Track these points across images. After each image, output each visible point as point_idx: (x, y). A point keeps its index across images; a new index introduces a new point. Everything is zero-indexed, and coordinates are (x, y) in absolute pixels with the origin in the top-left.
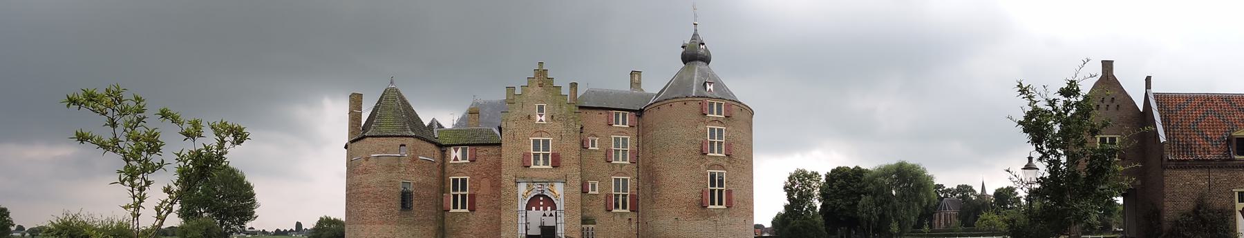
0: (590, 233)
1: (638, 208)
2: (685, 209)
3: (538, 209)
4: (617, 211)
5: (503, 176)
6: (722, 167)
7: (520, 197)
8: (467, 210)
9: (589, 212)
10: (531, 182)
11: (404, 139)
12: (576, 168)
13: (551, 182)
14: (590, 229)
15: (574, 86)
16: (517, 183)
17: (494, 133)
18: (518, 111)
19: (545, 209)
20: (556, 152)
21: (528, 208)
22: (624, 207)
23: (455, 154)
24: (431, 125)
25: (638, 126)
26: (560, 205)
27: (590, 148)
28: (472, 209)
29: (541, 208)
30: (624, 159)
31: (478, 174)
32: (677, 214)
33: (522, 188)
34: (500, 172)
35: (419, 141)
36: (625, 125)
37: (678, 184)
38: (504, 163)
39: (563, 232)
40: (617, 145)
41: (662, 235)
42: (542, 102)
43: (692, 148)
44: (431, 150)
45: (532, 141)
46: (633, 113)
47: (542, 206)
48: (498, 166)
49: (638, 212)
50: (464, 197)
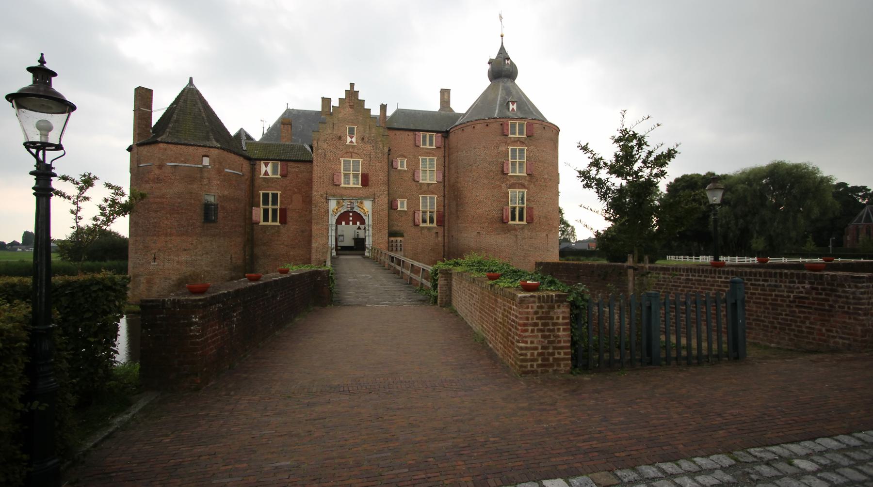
0: (399, 244)
2: (486, 224)
3: (347, 223)
4: (424, 225)
6: (523, 186)
7: (330, 212)
9: (398, 226)
10: (340, 198)
11: (207, 150)
13: (361, 199)
14: (399, 241)
15: (383, 108)
16: (327, 200)
17: (305, 148)
21: (338, 222)
22: (431, 221)
25: (445, 147)
27: (399, 168)
29: (351, 223)
33: (333, 204)
35: (225, 153)
36: (432, 146)
37: (480, 202)
41: (466, 246)
44: (238, 162)
46: (440, 135)
47: (351, 221)
48: (309, 183)
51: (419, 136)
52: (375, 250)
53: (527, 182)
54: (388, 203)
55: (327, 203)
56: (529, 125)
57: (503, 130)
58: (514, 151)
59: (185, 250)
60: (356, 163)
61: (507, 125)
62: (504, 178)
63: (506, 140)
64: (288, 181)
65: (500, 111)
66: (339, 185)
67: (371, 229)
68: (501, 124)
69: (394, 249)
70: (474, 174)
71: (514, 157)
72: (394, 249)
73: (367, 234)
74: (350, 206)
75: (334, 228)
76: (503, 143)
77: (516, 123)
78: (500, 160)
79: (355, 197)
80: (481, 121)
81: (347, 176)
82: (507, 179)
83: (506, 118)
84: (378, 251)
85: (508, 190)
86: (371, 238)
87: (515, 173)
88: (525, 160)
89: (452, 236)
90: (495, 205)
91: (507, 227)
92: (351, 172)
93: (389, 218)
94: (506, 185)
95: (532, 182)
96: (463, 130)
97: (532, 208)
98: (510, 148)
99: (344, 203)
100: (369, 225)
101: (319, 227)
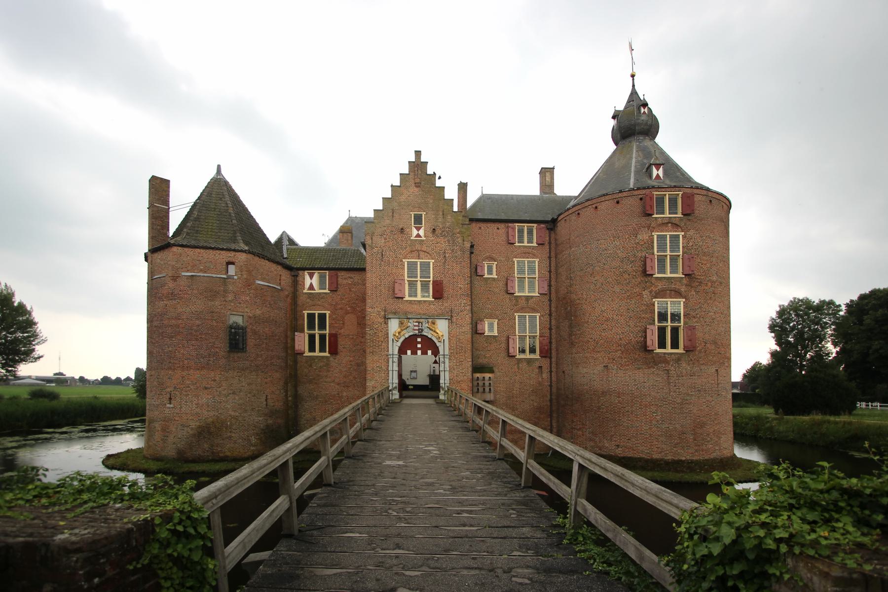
1: (551, 353)
3: (414, 353)
5: (369, 310)
6: (678, 294)
7: (391, 337)
8: (327, 354)
10: (404, 317)
12: (465, 301)
13: (433, 318)
15: (463, 188)
16: (386, 319)
18: (388, 222)
19: (424, 353)
20: (439, 279)
21: (402, 351)
22: (533, 350)
23: (311, 281)
24: (280, 241)
26: (444, 348)
28: (334, 351)
29: (419, 352)
30: (532, 288)
31: (341, 309)
32: (606, 360)
33: (394, 326)
34: (365, 305)
37: (607, 320)
38: (369, 292)
39: (447, 381)
40: (521, 271)
42: (420, 209)
43: (629, 268)
44: (275, 273)
45: (406, 263)
47: (419, 349)
49: (551, 358)
50: (323, 337)
51: (514, 229)
52: (452, 391)
53: (684, 287)
54: (472, 324)
55: (386, 323)
56: (688, 200)
57: (644, 207)
58: (662, 238)
59: (206, 388)
60: (424, 266)
61: (651, 198)
62: (646, 282)
63: (648, 222)
64: (339, 297)
65: (636, 180)
66: (403, 298)
67: (447, 361)
68: (641, 199)
69: (481, 389)
70: (596, 278)
71: (662, 247)
72: (481, 389)
73: (442, 369)
74: (417, 328)
75: (396, 360)
76: (645, 227)
77: (665, 195)
78: (639, 254)
79: (424, 314)
80: (607, 198)
81: (412, 285)
82: (651, 283)
83: (648, 188)
84: (456, 394)
85: (654, 300)
86: (447, 374)
87: (664, 273)
88: (681, 253)
89: (564, 372)
90: (631, 323)
91: (653, 358)
92: (419, 278)
93: (472, 345)
94: (651, 292)
95: (692, 287)
96: (579, 214)
97: (694, 328)
98: (655, 235)
99: (409, 324)
100: (444, 355)
101: (376, 358)
